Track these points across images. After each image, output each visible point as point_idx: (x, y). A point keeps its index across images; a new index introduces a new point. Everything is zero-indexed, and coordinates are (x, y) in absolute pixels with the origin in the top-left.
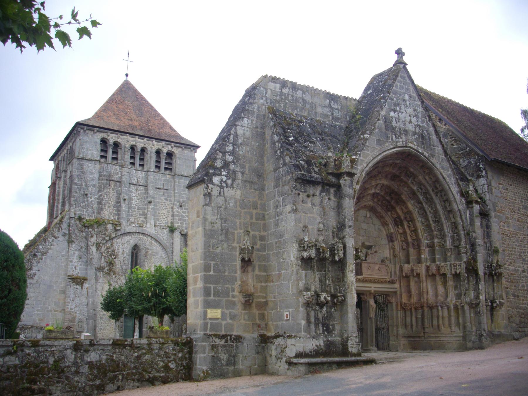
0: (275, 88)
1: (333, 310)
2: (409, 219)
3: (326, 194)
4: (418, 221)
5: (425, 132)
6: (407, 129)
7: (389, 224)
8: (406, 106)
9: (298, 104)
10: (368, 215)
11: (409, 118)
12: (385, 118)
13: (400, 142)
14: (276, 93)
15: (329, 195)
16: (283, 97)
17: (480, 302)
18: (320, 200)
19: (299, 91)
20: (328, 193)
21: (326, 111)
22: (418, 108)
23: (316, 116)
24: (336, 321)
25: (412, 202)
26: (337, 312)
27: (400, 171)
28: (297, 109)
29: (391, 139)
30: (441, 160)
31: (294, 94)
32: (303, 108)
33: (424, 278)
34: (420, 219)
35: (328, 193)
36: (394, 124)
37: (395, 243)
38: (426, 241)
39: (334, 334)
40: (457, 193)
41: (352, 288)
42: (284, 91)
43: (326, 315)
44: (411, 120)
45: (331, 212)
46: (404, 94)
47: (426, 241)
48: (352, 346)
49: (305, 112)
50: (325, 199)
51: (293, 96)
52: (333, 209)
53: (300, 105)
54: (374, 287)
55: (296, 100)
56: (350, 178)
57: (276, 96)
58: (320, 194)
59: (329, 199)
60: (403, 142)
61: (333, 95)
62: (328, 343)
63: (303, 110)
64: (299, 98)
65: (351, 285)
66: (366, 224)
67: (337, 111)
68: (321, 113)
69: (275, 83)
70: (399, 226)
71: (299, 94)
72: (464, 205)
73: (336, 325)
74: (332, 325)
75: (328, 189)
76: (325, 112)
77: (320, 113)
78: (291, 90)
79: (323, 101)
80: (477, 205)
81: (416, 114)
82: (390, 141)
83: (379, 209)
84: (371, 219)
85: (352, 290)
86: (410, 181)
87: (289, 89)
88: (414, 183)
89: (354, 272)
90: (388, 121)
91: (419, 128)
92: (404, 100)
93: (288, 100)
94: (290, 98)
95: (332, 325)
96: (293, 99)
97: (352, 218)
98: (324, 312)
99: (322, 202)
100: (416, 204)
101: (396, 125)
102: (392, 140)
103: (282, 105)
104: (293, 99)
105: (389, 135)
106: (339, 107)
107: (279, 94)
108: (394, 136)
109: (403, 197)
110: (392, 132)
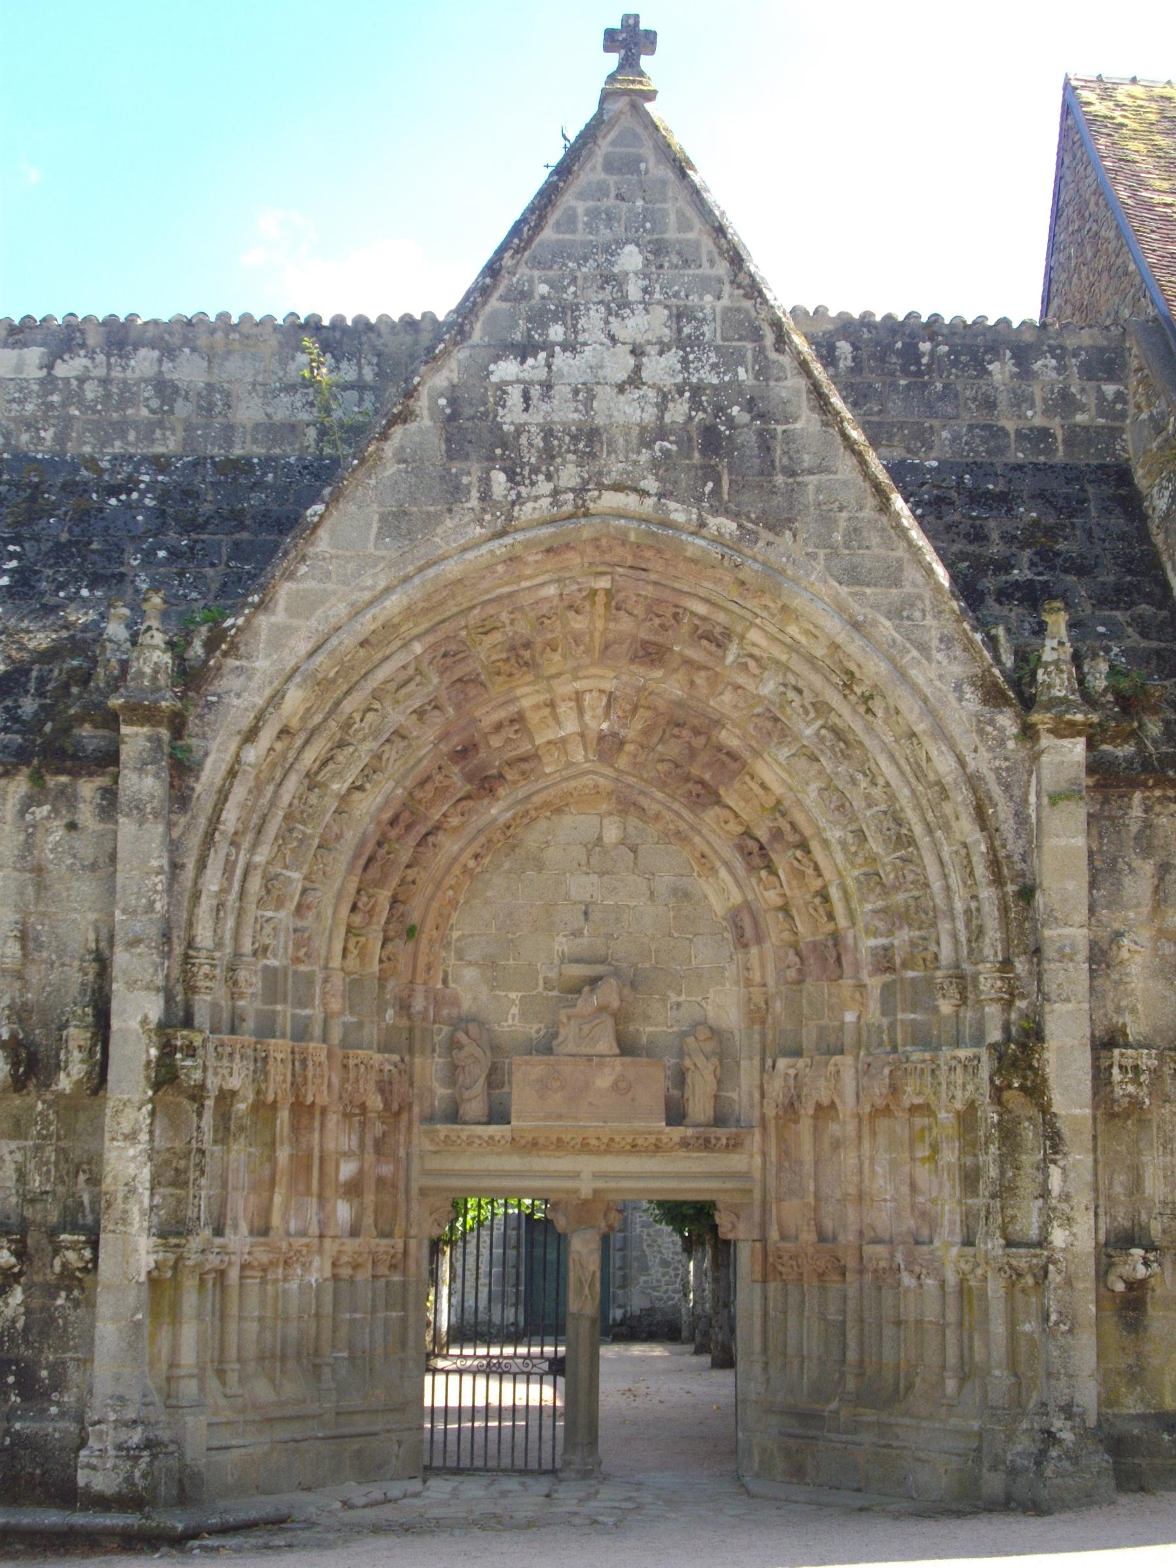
0: (19, 367)
1: (60, 1302)
2: (792, 838)
3: (55, 810)
4: (825, 843)
5: (735, 410)
6: (600, 421)
7: (718, 864)
8: (620, 306)
9: (130, 412)
10: (612, 834)
11: (631, 361)
12: (452, 402)
13: (537, 498)
14: (21, 390)
15: (72, 807)
16: (55, 398)
17: (1050, 1260)
18: (22, 838)
19: (143, 352)
20: (67, 798)
21: (285, 409)
22: (708, 298)
23: (230, 444)
24: (75, 1348)
25: (785, 752)
26: (80, 1312)
27: (657, 621)
28: (123, 436)
29: (475, 494)
30: (838, 537)
31: (117, 373)
32: (160, 424)
33: (851, 1128)
34: (838, 833)
35: (67, 798)
36: (511, 415)
37: (754, 951)
38: (873, 942)
39: (58, 1404)
40: (958, 688)
41: (125, 1212)
42: (61, 370)
43: (20, 1325)
44: (638, 369)
45: (76, 884)
46: (611, 250)
47: (873, 942)
48: (94, 1461)
49: (165, 438)
50: (48, 832)
51: (105, 382)
52: (94, 867)
53: (144, 412)
54: (596, 1176)
55: (127, 396)
56: (145, 730)
57: (21, 402)
58: (22, 813)
59: (72, 826)
60: (556, 492)
61: (338, 322)
62: (8, 1441)
63: (158, 434)
64: (137, 384)
65: (120, 1195)
66: (594, 878)
67: (353, 395)
68: (257, 426)
69: (24, 345)
70: (763, 873)
71: (144, 362)
72: (1011, 745)
73: (71, 1366)
74: (52, 1367)
75: (65, 786)
76: (280, 416)
77: (249, 425)
78: (101, 358)
79: (275, 365)
80: (1066, 742)
81: (687, 330)
82: (474, 503)
83: (655, 800)
84: (634, 850)
85: (124, 1220)
86: (730, 658)
87: (91, 356)
88: (752, 664)
89: (144, 1137)
90: (468, 411)
91: (693, 397)
92: (608, 279)
93: (81, 402)
94: (90, 396)
95: (52, 1367)
96: (108, 396)
97: (152, 903)
98: (9, 1312)
99: (29, 846)
100: (803, 763)
101: (525, 417)
102: (485, 496)
103: (48, 435)
104: (108, 396)
105: (465, 480)
106: (368, 374)
107: (36, 388)
108: (499, 478)
109: (729, 738)
110: (492, 458)
